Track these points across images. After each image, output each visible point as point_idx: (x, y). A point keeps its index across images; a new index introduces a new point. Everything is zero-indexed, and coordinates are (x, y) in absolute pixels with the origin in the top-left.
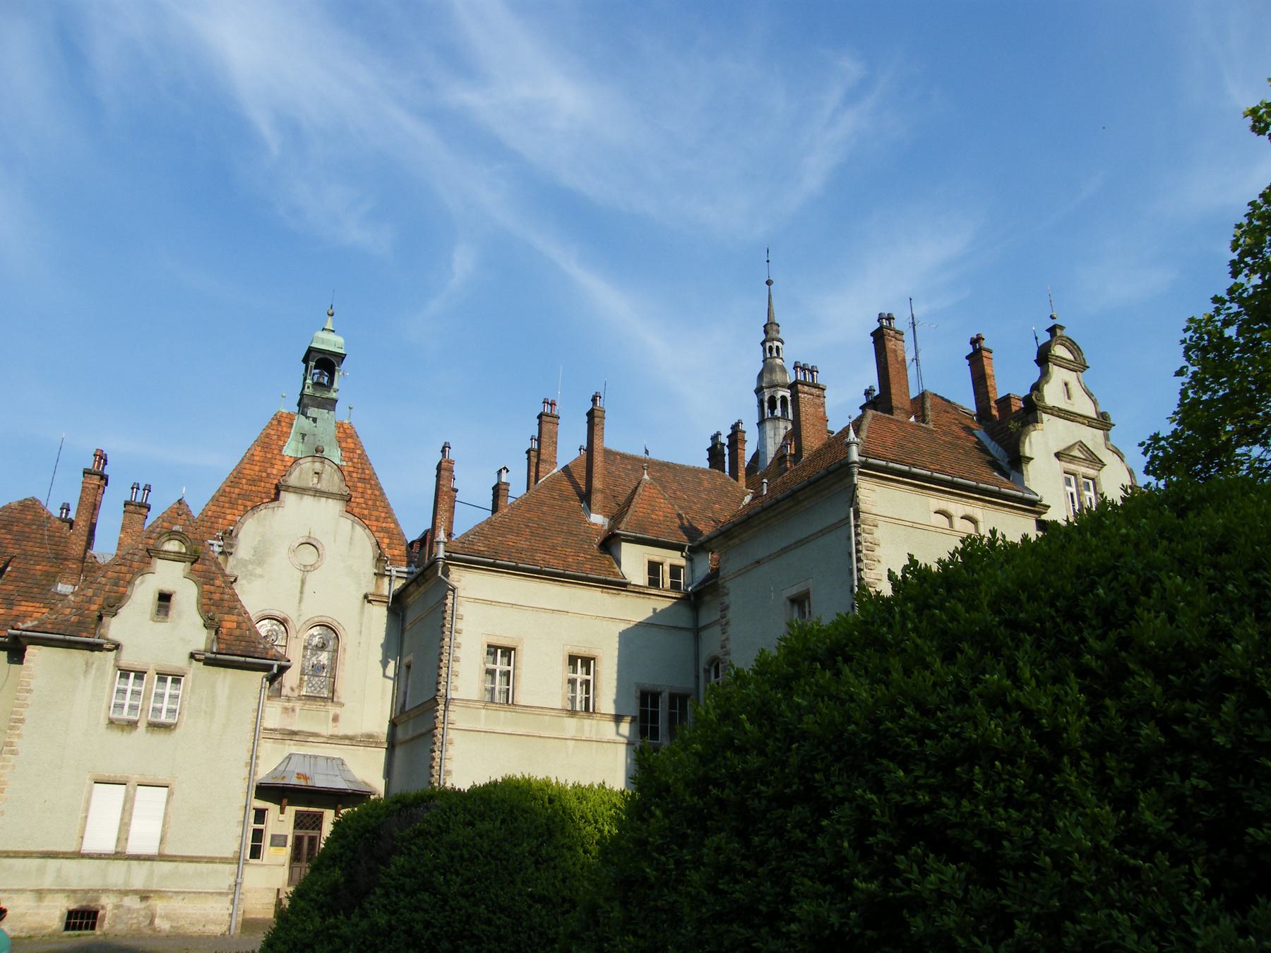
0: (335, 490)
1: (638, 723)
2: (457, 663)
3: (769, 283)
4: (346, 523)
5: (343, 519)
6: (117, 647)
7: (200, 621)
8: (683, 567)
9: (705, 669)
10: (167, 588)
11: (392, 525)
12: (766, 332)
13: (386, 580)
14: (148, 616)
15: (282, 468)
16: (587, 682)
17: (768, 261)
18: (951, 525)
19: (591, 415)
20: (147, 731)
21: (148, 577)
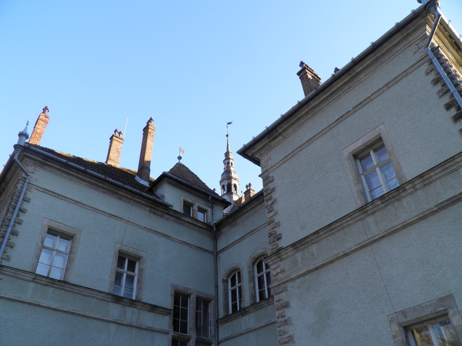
1: (172, 316)
2: (15, 237)
3: (227, 136)
9: (223, 280)
17: (227, 127)
19: (146, 130)
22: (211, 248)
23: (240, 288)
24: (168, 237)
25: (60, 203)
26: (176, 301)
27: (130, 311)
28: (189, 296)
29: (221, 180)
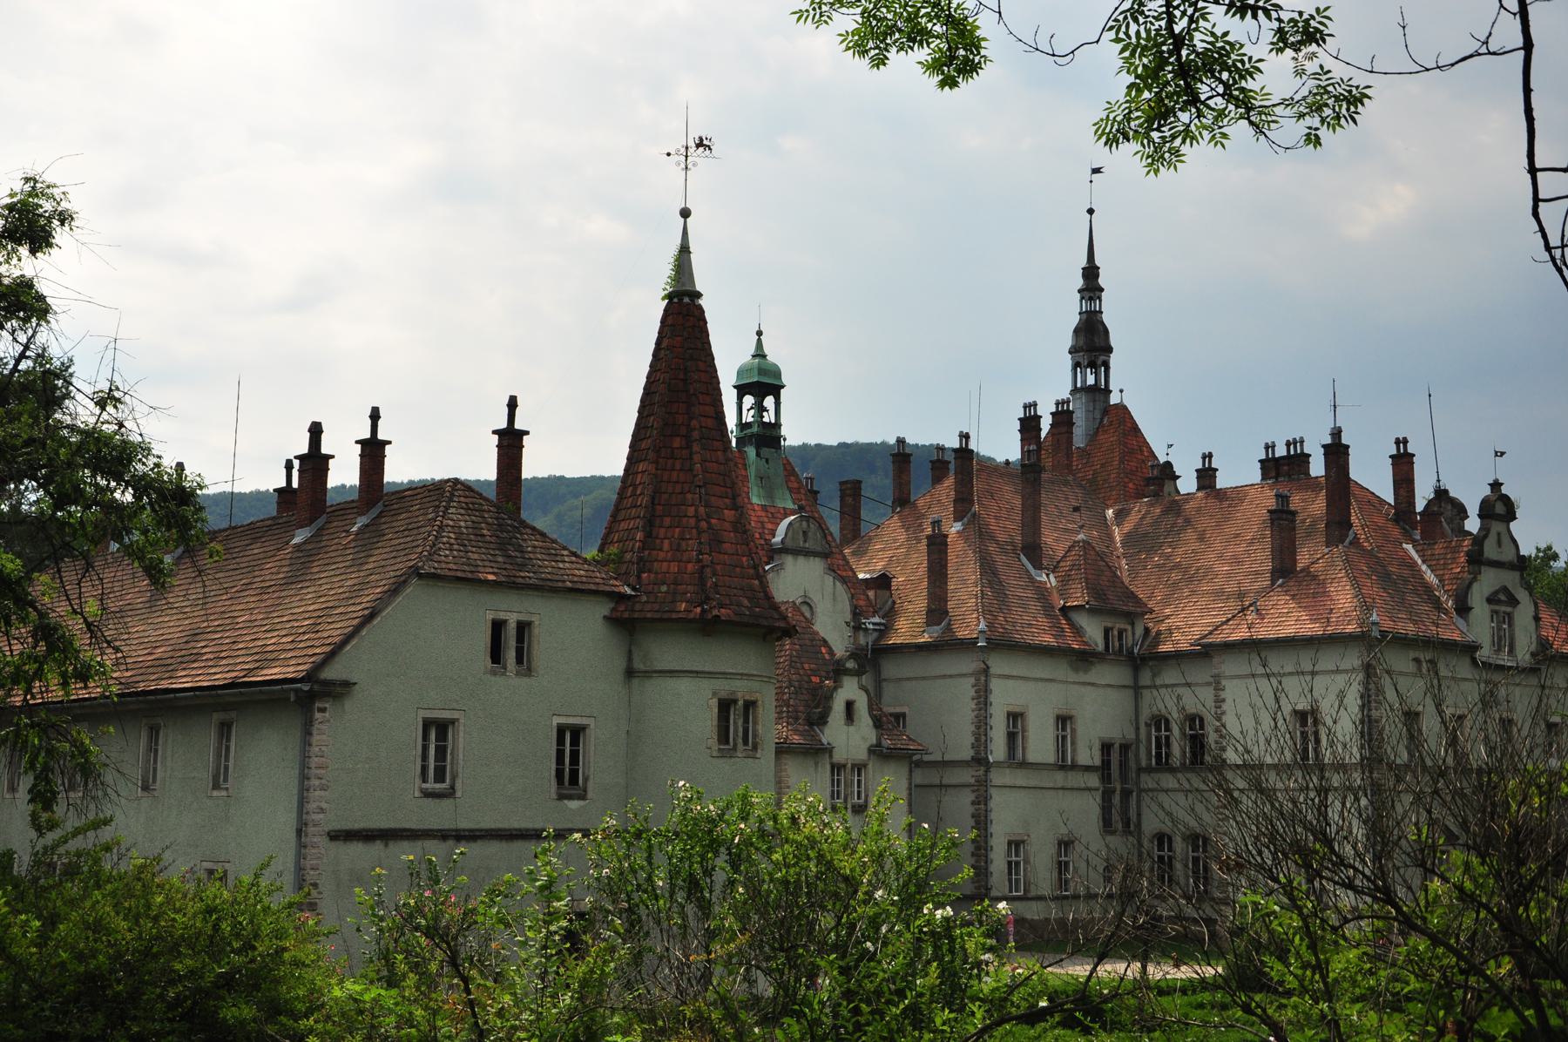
0: (819, 549)
3: (1091, 211)
4: (829, 580)
5: (826, 577)
6: (828, 750)
7: (870, 722)
8: (1126, 630)
9: (1146, 723)
10: (851, 697)
11: (850, 573)
12: (1084, 276)
13: (861, 633)
14: (843, 722)
15: (755, 519)
16: (1064, 738)
17: (1091, 182)
18: (1420, 669)
20: (853, 811)
21: (840, 690)
22: (1132, 684)
23: (1167, 738)
24: (1093, 684)
25: (1010, 683)
26: (1103, 754)
27: (1070, 774)
28: (1113, 745)
29: (1072, 347)
